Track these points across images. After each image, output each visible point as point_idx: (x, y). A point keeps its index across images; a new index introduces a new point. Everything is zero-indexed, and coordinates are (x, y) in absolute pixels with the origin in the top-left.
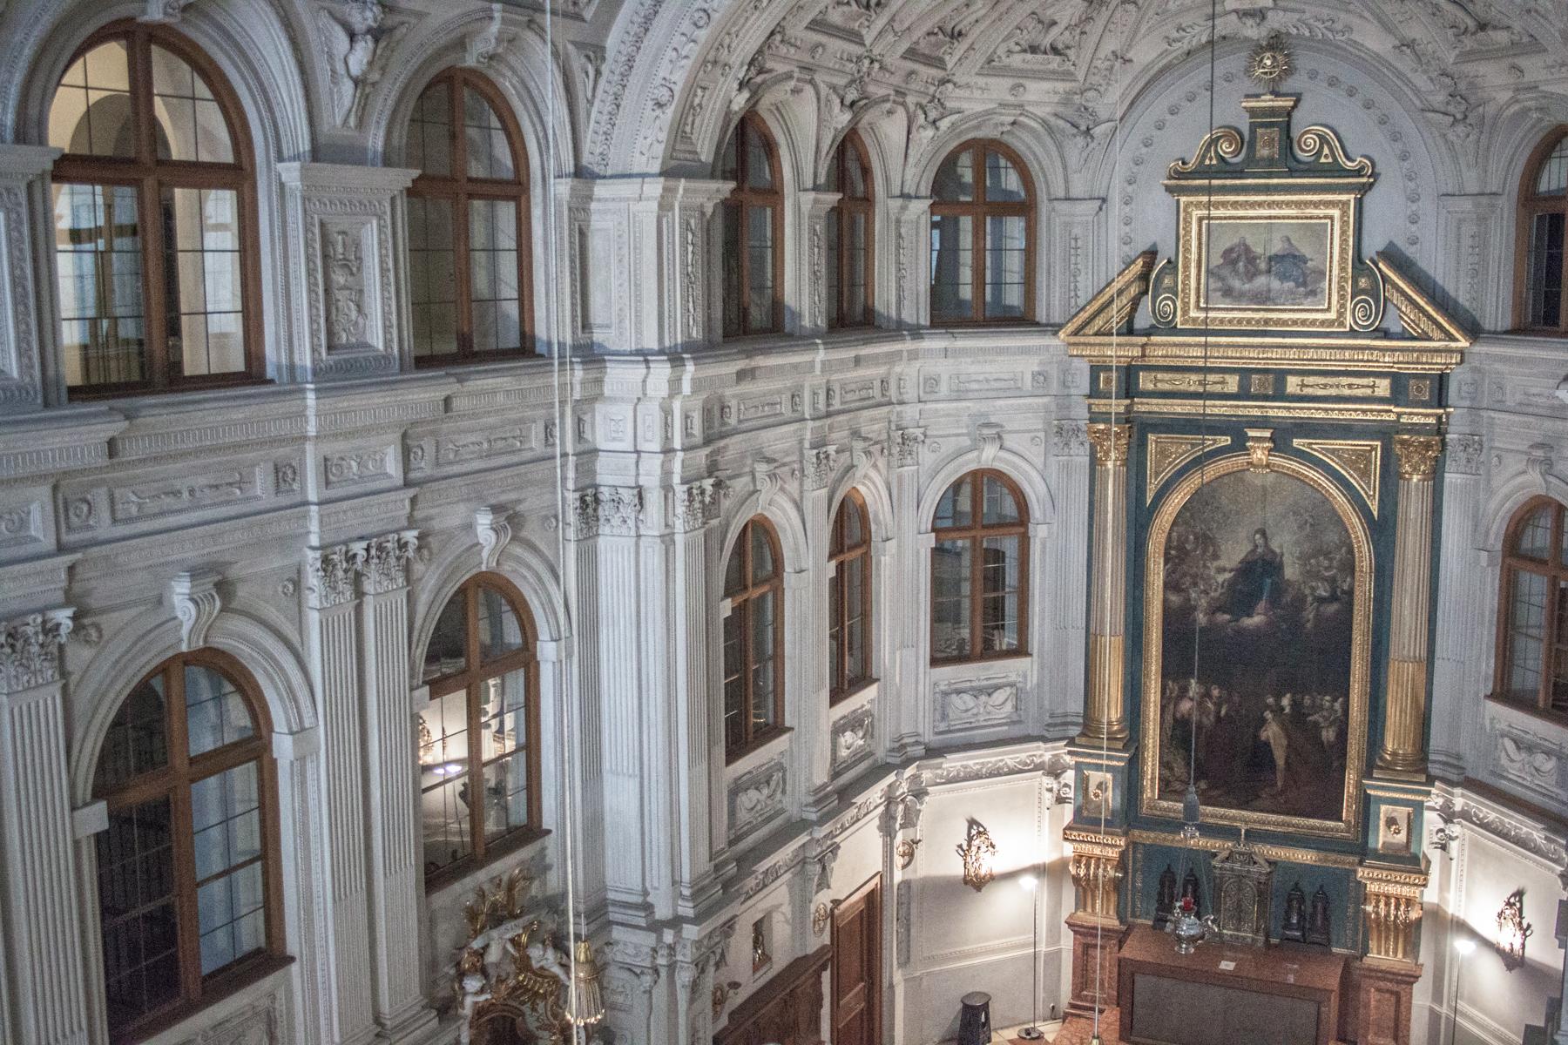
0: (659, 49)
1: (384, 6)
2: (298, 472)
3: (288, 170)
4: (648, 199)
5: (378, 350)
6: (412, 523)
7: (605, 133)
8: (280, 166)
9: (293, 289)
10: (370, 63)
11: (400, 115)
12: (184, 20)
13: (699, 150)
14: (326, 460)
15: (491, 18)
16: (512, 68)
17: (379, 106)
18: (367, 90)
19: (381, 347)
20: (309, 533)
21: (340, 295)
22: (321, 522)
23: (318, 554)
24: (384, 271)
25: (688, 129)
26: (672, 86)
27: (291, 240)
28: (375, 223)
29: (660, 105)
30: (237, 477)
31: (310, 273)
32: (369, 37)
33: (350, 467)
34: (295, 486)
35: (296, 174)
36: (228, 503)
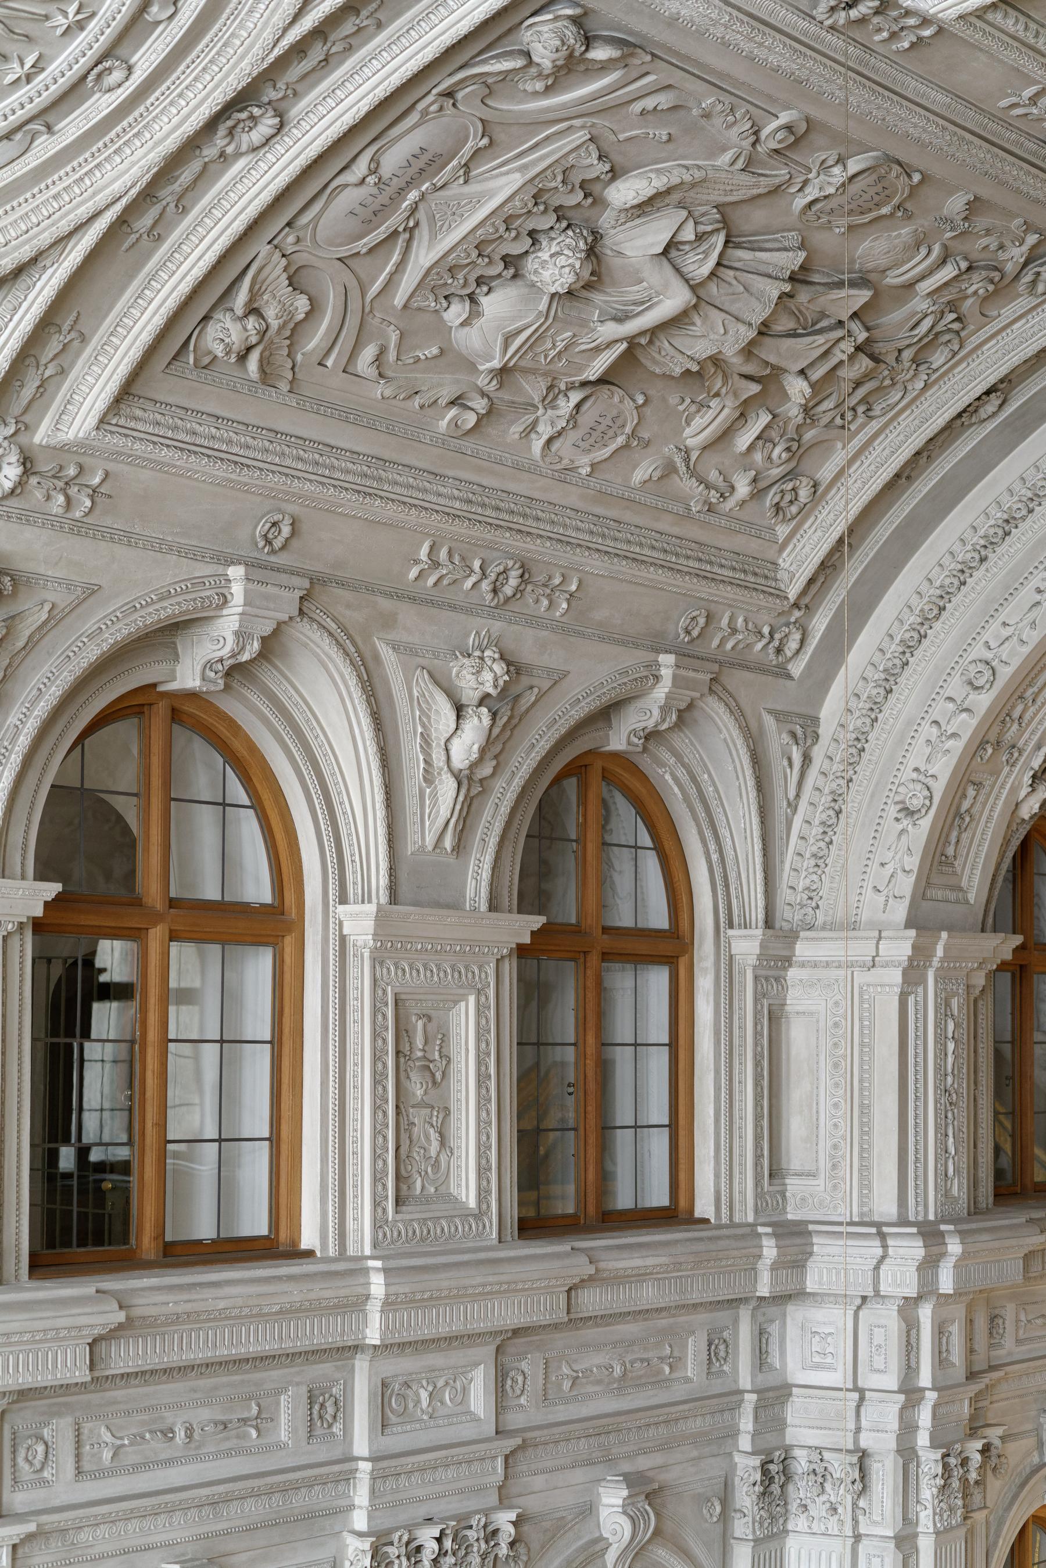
0: (909, 723)
1: (509, 664)
2: (342, 1407)
3: (355, 916)
4: (886, 965)
5: (464, 1206)
6: (504, 1501)
7: (814, 855)
8: (341, 908)
9: (350, 1104)
10: (483, 751)
11: (511, 835)
12: (227, 687)
13: (964, 884)
14: (384, 1385)
15: (657, 678)
16: (679, 757)
17: (487, 814)
18: (476, 789)
19: (472, 1203)
20: (351, 1507)
21: (418, 1117)
22: (373, 1491)
23: (366, 1544)
24: (482, 1079)
25: (950, 851)
26: (930, 782)
27: (351, 1029)
28: (472, 999)
29: (909, 812)
30: (255, 1410)
31: (378, 1080)
32: (484, 710)
33: (418, 1402)
34: (337, 1429)
35: (369, 925)
36: (239, 1452)
